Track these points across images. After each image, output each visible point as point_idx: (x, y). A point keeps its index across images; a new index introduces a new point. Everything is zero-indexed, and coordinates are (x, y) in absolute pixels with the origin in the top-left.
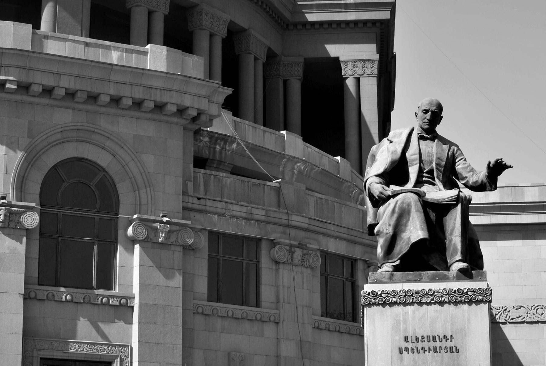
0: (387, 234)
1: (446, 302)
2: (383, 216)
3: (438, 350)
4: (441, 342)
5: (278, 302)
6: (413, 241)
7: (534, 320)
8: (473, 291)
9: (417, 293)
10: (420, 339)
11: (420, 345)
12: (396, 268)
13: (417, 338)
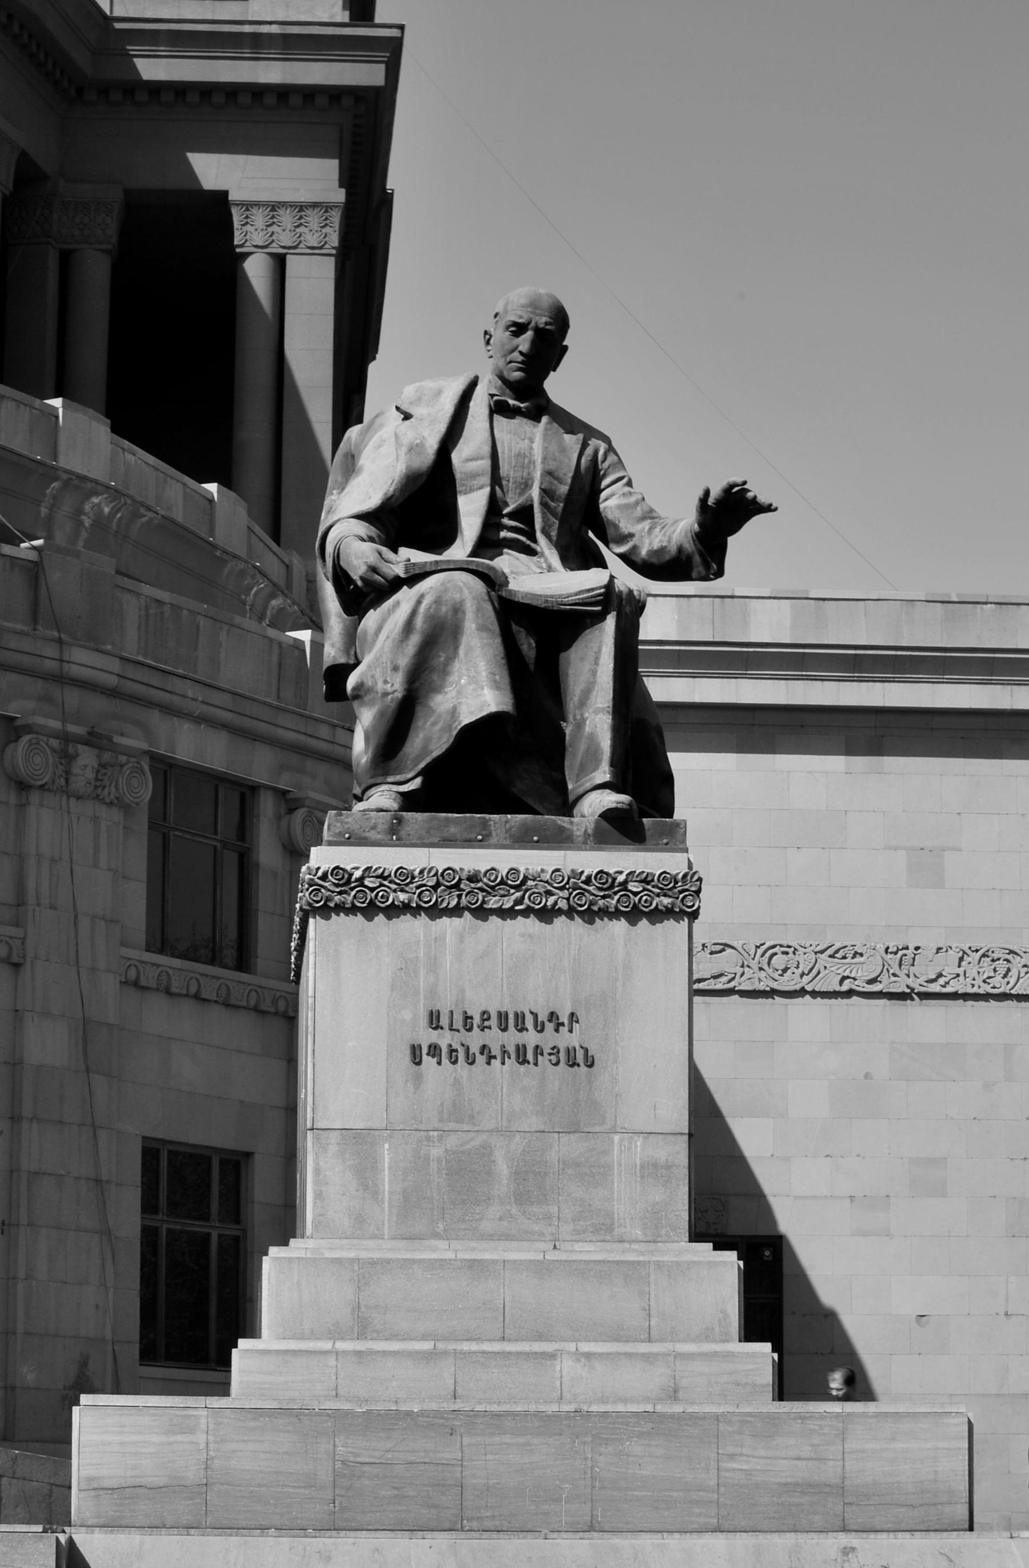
0: (386, 694)
1: (560, 912)
2: (374, 641)
3: (530, 1057)
4: (541, 1031)
5: (20, 902)
6: (467, 718)
7: (761, 987)
8: (645, 881)
9: (473, 878)
10: (477, 1020)
11: (475, 1040)
12: (410, 802)
13: (467, 1018)
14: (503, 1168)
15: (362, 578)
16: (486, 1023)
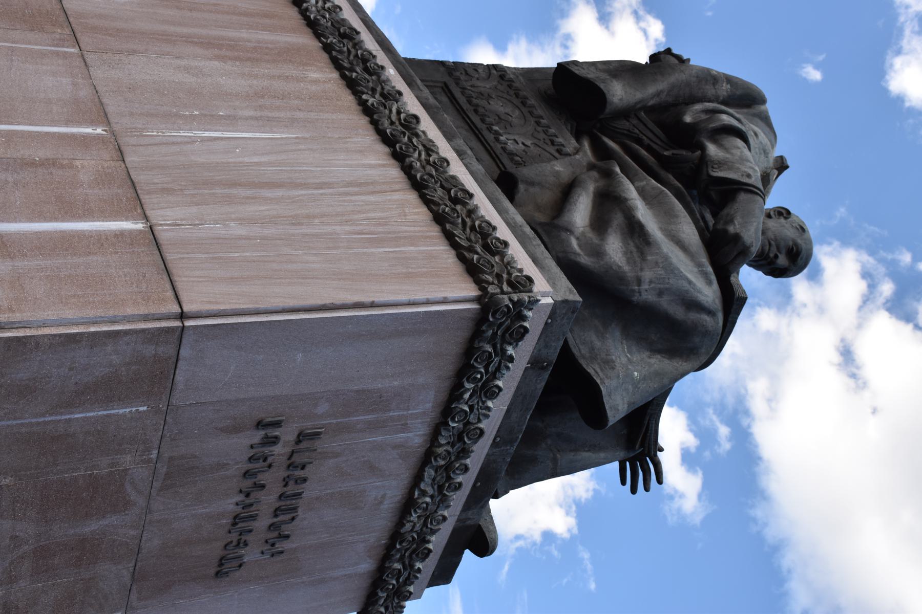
9: (465, 452)
10: (299, 473)
11: (272, 479)
14: (92, 527)
16: (291, 483)
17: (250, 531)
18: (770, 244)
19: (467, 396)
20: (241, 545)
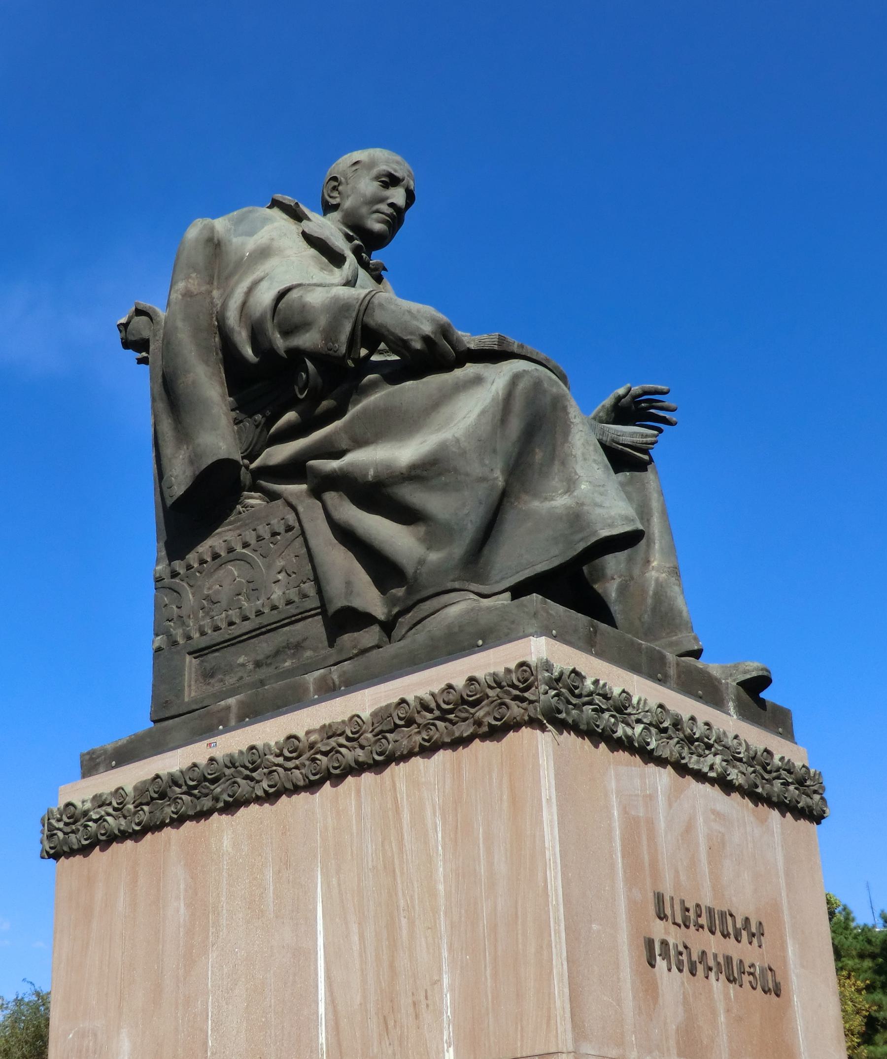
10: (692, 914)
15: (426, 339)
17: (741, 961)
18: (377, 211)
19: (629, 731)
20: (752, 970)
